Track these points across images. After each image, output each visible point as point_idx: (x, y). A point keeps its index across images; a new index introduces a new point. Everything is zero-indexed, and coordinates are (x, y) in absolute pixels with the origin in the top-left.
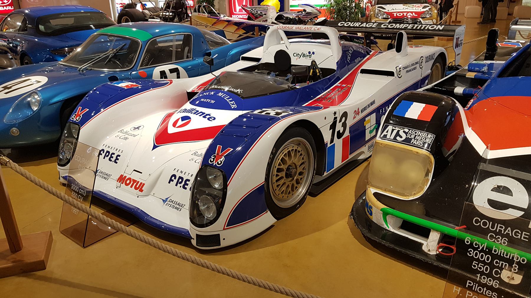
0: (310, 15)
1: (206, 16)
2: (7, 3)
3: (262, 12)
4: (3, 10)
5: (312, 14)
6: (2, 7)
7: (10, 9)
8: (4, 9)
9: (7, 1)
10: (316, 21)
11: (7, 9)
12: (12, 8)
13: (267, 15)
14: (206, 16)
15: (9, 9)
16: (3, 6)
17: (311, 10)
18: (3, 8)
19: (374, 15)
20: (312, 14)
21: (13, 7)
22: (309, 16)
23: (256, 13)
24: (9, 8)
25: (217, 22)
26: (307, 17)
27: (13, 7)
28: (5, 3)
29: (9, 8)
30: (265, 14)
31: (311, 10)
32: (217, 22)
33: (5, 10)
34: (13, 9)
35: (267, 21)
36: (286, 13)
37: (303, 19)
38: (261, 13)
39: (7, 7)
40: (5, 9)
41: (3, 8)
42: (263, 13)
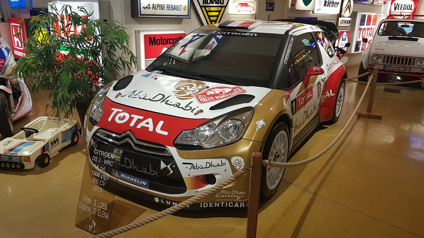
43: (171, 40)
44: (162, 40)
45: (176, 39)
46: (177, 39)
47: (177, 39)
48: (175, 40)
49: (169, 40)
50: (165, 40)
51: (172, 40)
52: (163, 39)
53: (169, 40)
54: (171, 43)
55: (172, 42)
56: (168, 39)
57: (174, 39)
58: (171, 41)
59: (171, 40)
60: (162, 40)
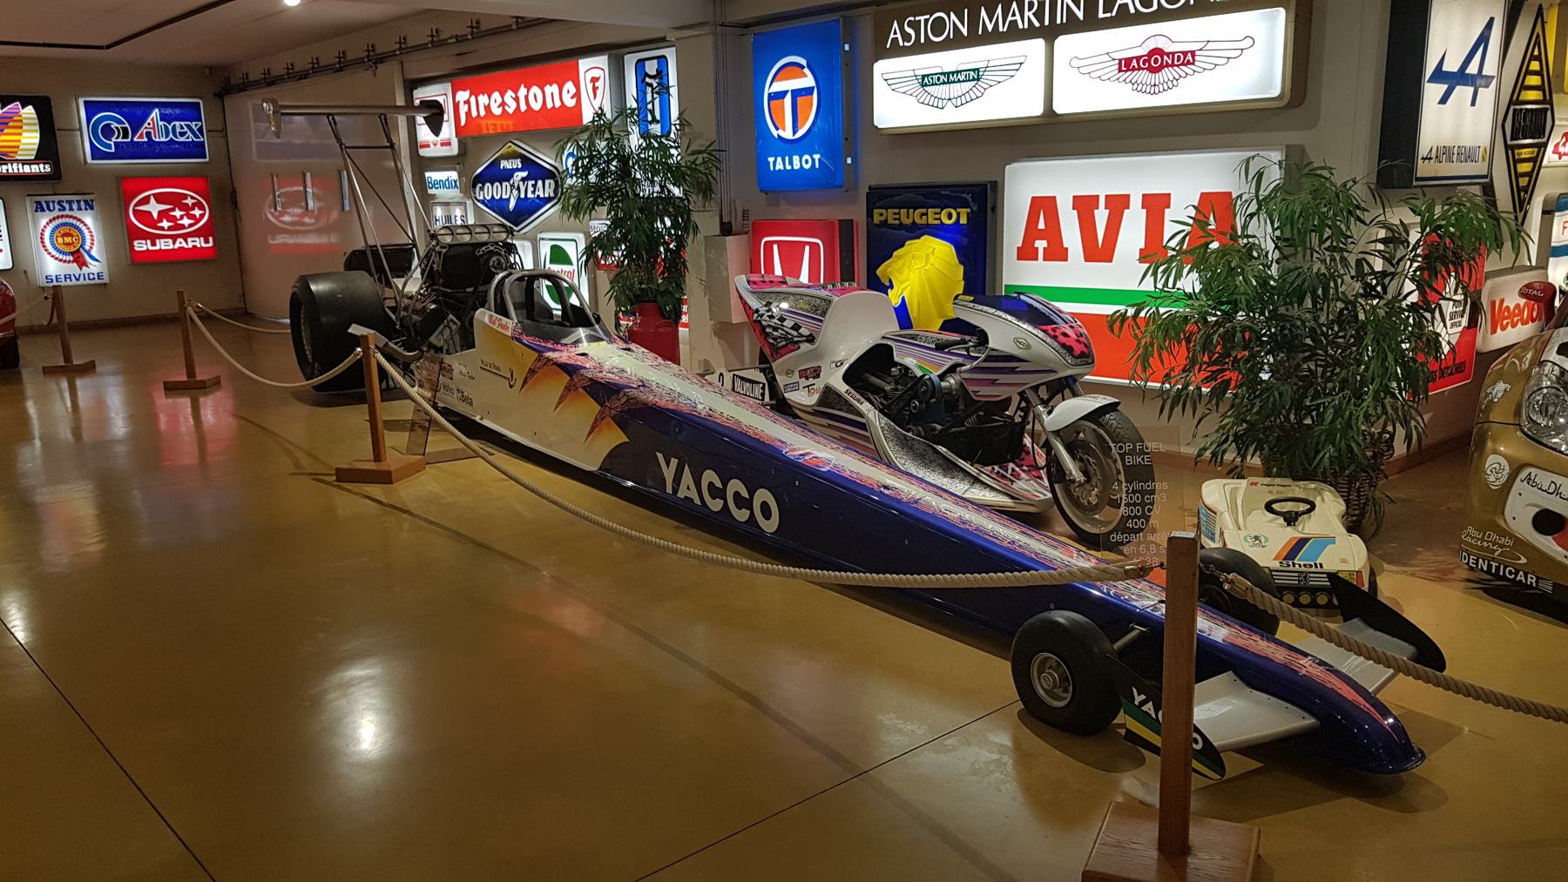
0: (1013, 371)
1: (509, 333)
2: (190, 226)
3: (801, 320)
4: (173, 250)
5: (1022, 366)
6: (170, 241)
7: (199, 246)
8: (176, 246)
9: (192, 221)
10: (1049, 413)
11: (186, 246)
12: (207, 241)
13: (817, 343)
14: (509, 333)
15: (195, 247)
16: (174, 238)
17: (1017, 341)
18: (174, 243)
19: (1518, 413)
20: (1022, 366)
21: (211, 239)
22: (1003, 378)
23: (775, 329)
24: (199, 242)
25: (539, 368)
26: (993, 383)
27: (211, 239)
28: (183, 227)
29: (194, 244)
30: (811, 339)
31: (1017, 341)
32: (539, 368)
33: (181, 249)
34: (211, 244)
35: (818, 376)
36: (913, 337)
37: (975, 392)
38: (796, 327)
39: (189, 240)
40: (181, 245)
41: (174, 243)
42: (801, 331)
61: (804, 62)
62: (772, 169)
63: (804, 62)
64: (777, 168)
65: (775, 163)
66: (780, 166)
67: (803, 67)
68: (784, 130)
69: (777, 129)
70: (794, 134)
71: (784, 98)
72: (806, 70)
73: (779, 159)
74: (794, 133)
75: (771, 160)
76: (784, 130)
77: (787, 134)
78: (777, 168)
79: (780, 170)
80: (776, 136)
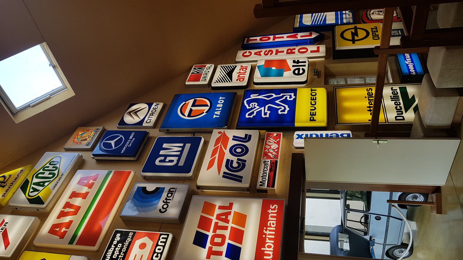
43: (264, 170)
44: (264, 176)
45: (265, 166)
46: (265, 165)
47: (265, 165)
48: (265, 167)
49: (264, 171)
50: (264, 174)
51: (265, 169)
52: (262, 176)
53: (264, 171)
54: (267, 170)
55: (266, 169)
56: (263, 172)
57: (264, 167)
58: (266, 169)
59: (264, 170)
60: (264, 176)
61: (184, 103)
62: (219, 116)
63: (184, 103)
64: (219, 114)
65: (216, 115)
66: (219, 113)
67: (186, 103)
68: (204, 110)
69: (203, 113)
70: (209, 106)
71: (192, 110)
72: (187, 102)
73: (216, 113)
74: (208, 106)
75: (215, 116)
76: (204, 110)
77: (207, 108)
78: (219, 114)
79: (220, 113)
80: (206, 113)
